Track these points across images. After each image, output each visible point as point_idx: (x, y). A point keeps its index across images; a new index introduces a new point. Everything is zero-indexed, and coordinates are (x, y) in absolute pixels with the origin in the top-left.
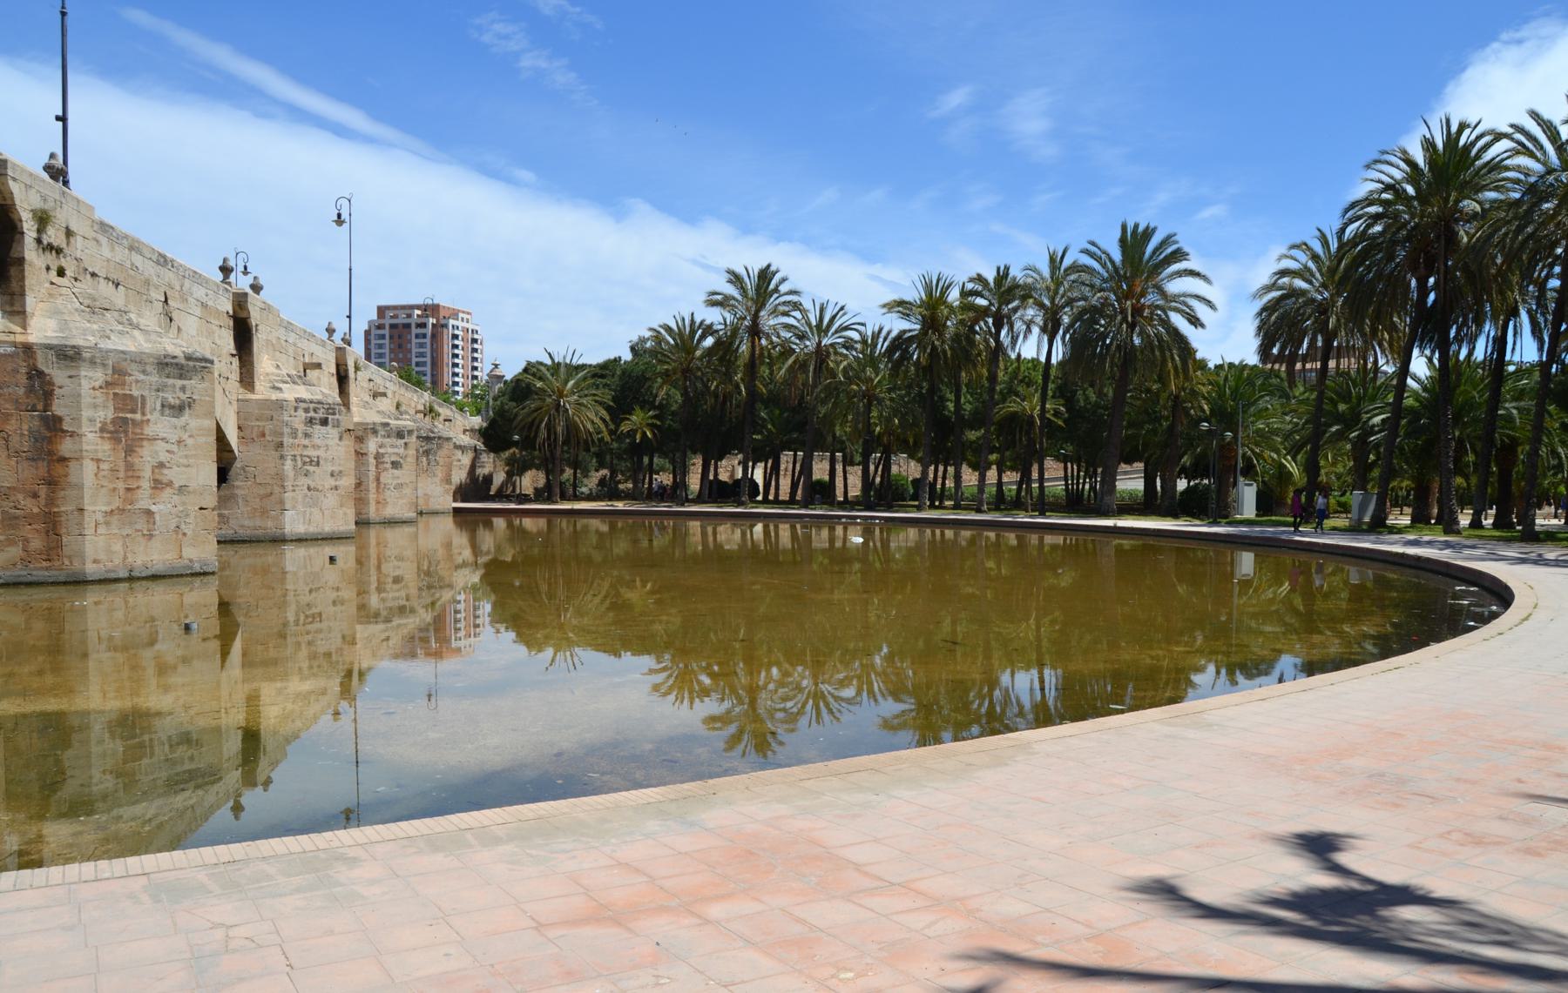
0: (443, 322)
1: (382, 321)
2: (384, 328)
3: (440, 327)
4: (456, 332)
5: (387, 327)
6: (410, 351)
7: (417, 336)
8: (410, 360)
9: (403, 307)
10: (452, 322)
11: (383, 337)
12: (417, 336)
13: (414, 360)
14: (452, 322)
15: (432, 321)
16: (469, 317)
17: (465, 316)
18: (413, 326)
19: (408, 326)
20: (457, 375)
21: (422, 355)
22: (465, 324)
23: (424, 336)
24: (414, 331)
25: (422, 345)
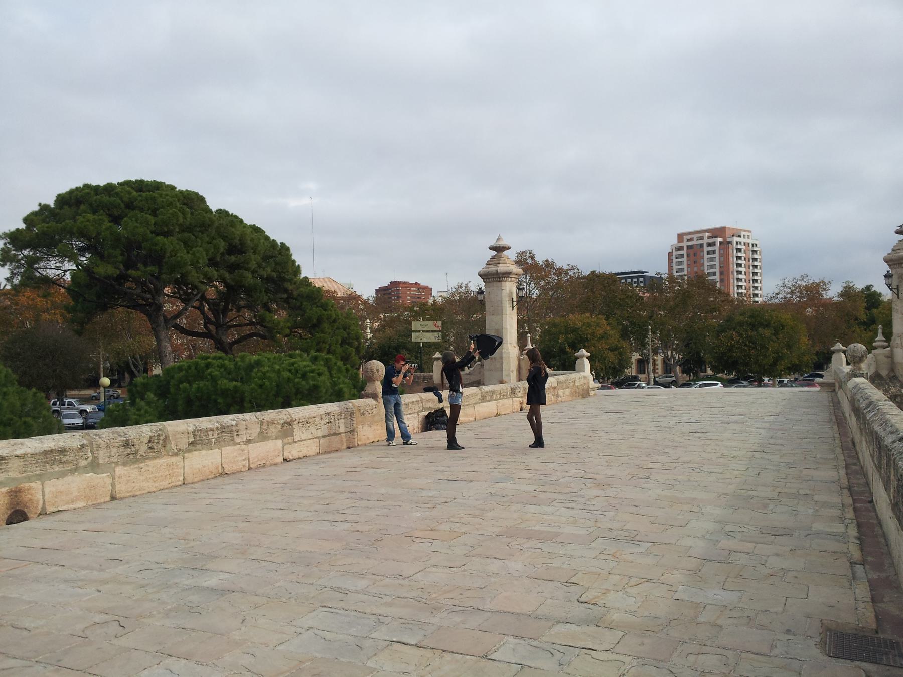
0: (728, 240)
1: (681, 245)
2: (683, 249)
3: (726, 244)
4: (739, 247)
5: (685, 248)
6: (703, 265)
7: (708, 253)
10: (736, 239)
11: (682, 256)
12: (708, 253)
15: (720, 239)
16: (749, 234)
17: (747, 234)
18: (705, 245)
19: (702, 245)
22: (746, 240)
23: (714, 252)
24: (706, 249)
25: (712, 259)
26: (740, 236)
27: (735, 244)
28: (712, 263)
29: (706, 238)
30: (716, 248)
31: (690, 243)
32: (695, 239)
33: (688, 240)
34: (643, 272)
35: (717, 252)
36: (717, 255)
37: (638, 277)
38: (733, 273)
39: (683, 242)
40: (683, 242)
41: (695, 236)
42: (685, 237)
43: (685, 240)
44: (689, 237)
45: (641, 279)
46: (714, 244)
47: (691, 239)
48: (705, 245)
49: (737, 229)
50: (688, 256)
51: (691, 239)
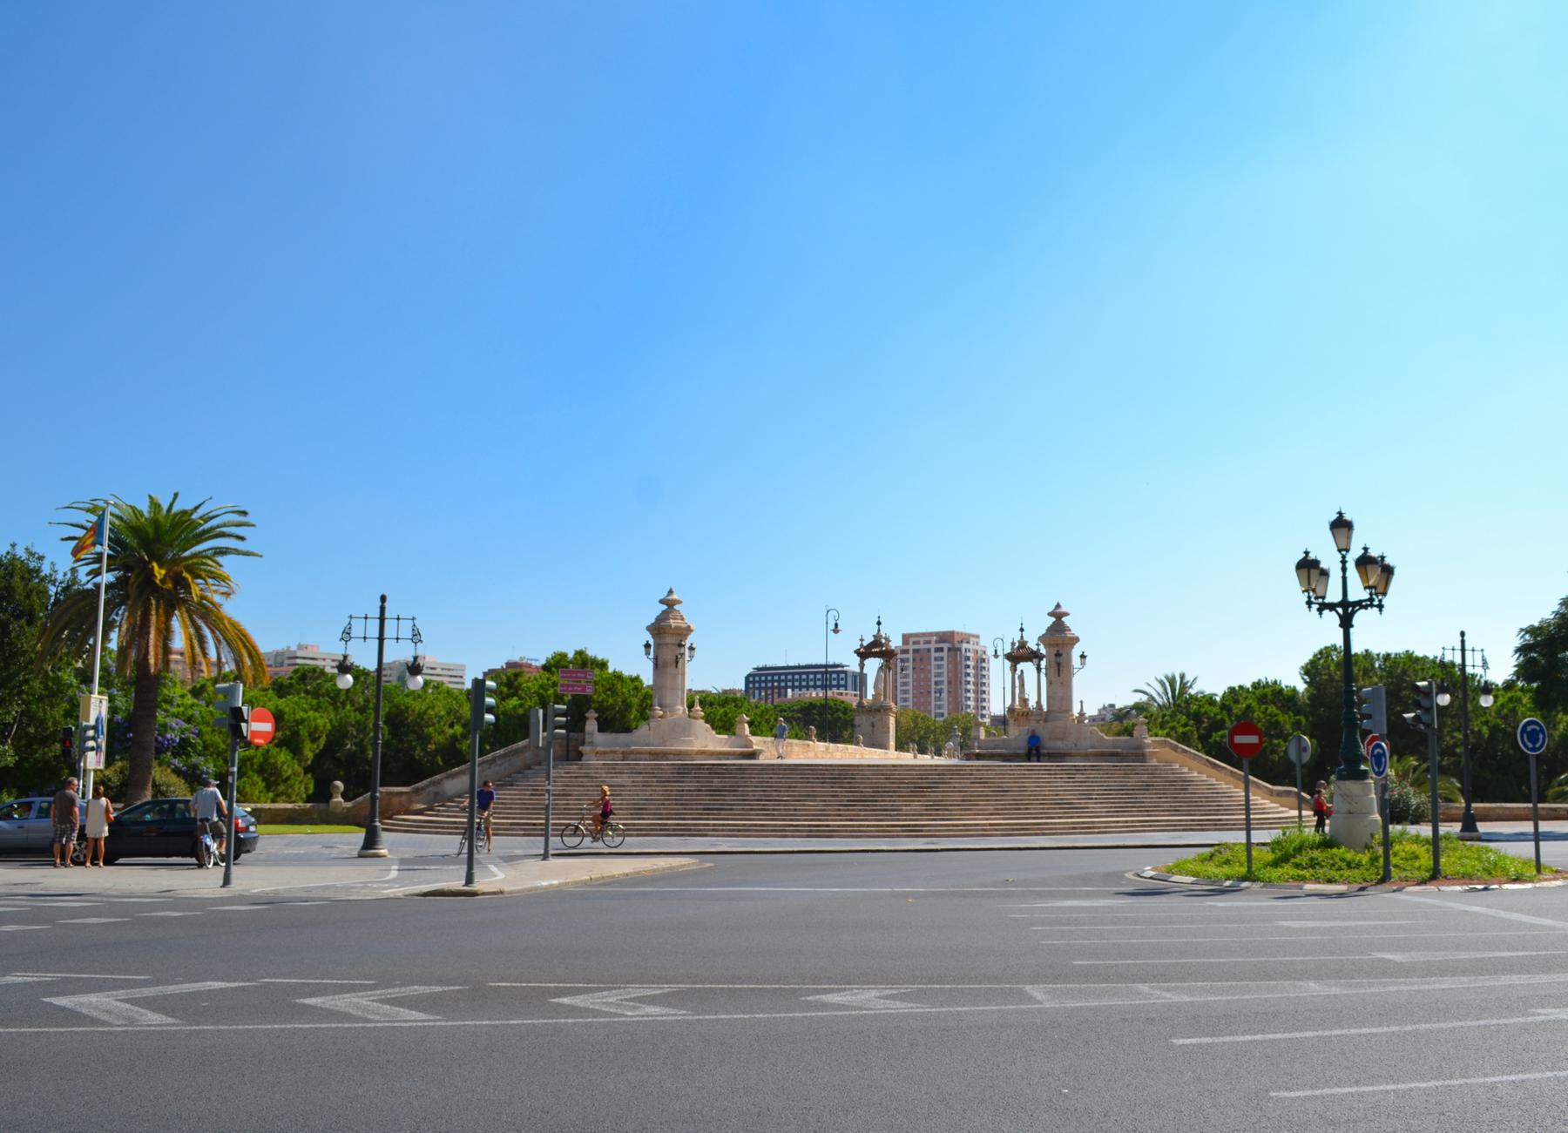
0: (957, 646)
1: (905, 647)
3: (954, 650)
4: (968, 654)
5: (911, 652)
6: (930, 672)
7: (936, 659)
8: (930, 680)
9: (924, 635)
10: (965, 646)
12: (936, 659)
13: (934, 679)
14: (965, 646)
17: (976, 640)
18: (933, 650)
20: (969, 691)
21: (939, 675)
22: (976, 647)
23: (942, 659)
24: (934, 655)
25: (939, 667)
26: (968, 642)
27: (964, 651)
28: (940, 671)
29: (933, 642)
30: (944, 654)
31: (917, 647)
32: (922, 642)
33: (914, 643)
34: (843, 667)
35: (945, 659)
36: (945, 662)
37: (838, 673)
38: (961, 683)
39: (908, 644)
40: (908, 644)
41: (922, 640)
42: (911, 640)
43: (911, 643)
44: (916, 639)
45: (842, 676)
46: (941, 650)
47: (918, 643)
48: (933, 650)
49: (965, 634)
50: (914, 660)
51: (918, 643)
